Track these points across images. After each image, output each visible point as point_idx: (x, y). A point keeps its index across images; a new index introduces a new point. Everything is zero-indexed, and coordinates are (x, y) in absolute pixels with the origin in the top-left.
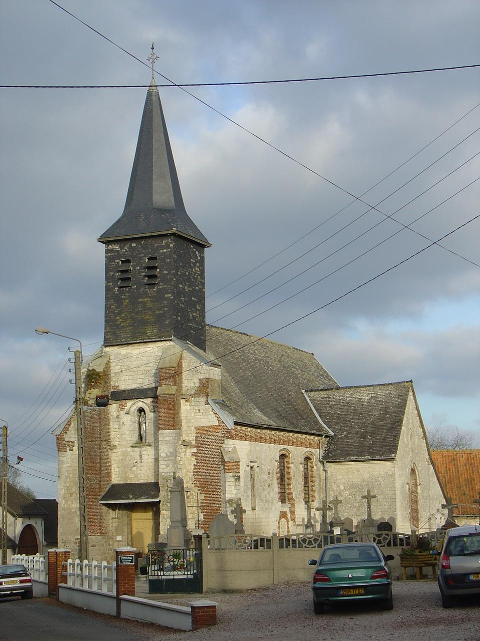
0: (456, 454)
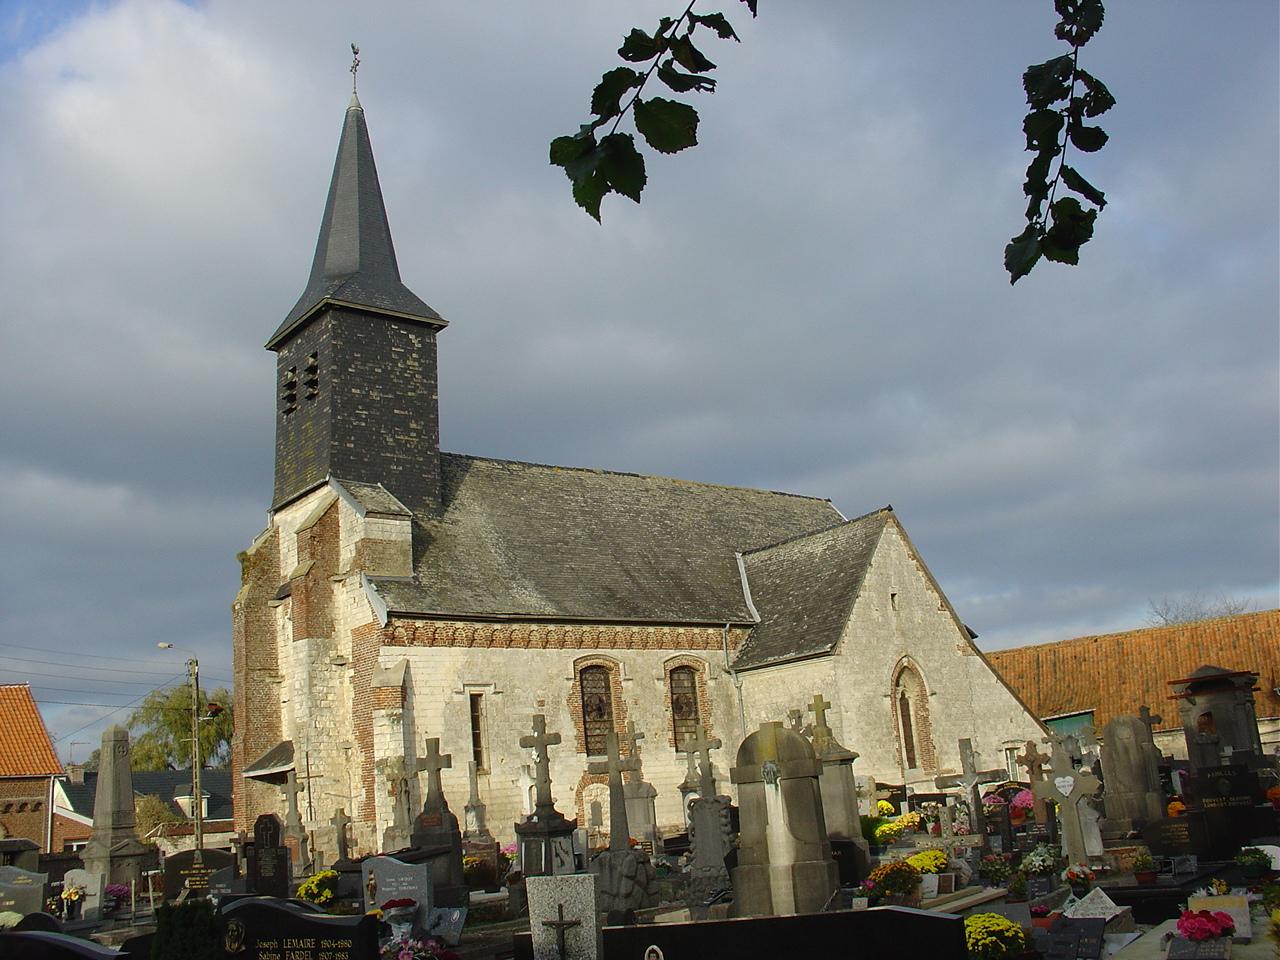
0: (1174, 632)
